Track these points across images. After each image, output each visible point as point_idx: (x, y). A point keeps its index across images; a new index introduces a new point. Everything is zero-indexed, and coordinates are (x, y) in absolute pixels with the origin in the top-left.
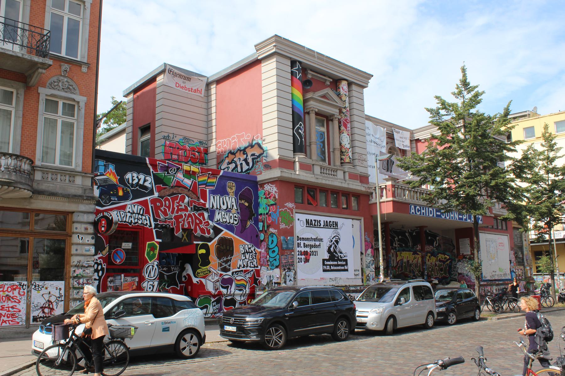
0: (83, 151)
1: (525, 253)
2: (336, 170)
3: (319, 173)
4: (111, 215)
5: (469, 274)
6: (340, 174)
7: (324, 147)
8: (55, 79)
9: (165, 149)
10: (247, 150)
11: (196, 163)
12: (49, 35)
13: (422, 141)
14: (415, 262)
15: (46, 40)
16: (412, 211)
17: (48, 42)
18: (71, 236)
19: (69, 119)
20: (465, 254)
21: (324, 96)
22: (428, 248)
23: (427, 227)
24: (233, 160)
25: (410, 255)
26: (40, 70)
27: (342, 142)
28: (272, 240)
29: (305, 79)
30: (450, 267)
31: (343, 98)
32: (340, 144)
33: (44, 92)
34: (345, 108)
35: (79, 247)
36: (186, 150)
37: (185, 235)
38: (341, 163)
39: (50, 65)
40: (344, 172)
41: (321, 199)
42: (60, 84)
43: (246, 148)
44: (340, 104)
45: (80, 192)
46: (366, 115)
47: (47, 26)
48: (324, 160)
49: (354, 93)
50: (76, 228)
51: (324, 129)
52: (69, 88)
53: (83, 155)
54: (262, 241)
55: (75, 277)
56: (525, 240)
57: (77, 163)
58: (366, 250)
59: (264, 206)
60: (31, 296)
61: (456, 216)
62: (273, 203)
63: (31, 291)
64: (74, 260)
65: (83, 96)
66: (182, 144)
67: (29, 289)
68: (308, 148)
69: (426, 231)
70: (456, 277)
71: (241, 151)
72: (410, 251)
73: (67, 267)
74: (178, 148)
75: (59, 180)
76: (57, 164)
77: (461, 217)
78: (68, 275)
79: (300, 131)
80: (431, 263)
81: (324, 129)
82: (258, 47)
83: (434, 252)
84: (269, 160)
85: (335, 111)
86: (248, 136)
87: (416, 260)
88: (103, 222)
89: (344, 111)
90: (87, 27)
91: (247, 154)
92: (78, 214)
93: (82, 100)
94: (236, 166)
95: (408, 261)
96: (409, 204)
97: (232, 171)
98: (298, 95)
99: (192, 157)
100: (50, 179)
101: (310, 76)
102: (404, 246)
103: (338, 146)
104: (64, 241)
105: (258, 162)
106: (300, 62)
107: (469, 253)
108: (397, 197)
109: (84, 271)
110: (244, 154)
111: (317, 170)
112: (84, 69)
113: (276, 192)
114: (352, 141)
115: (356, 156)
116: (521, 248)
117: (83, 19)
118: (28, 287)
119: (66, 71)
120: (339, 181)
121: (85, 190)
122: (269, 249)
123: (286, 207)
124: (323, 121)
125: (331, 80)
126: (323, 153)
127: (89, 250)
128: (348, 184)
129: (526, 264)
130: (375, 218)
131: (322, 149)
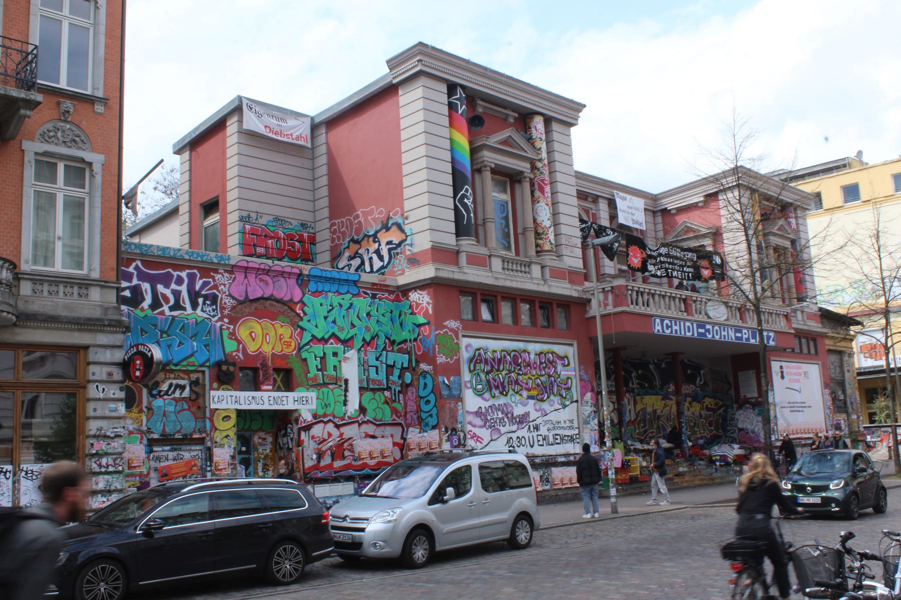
0: (102, 244)
1: (849, 391)
2: (530, 264)
3: (500, 270)
4: (150, 350)
5: (756, 429)
6: (536, 270)
7: (507, 226)
8: (50, 126)
9: (244, 238)
10: (379, 235)
11: (296, 259)
12: (35, 52)
13: (673, 212)
15: (32, 62)
17: (34, 65)
18: (85, 387)
19: (76, 192)
20: (749, 396)
21: (505, 142)
22: (687, 389)
23: (682, 353)
24: (357, 253)
26: (22, 112)
27: (537, 217)
28: (425, 384)
29: (472, 115)
30: (725, 419)
31: (538, 144)
32: (535, 220)
33: (32, 147)
34: (540, 160)
35: (99, 405)
36: (279, 239)
37: (279, 380)
38: (537, 252)
39: (39, 103)
40: (543, 267)
41: (505, 310)
42: (59, 134)
43: (377, 232)
44: (530, 154)
45: (97, 314)
46: (576, 172)
47: (35, 38)
48: (508, 248)
49: (556, 136)
50: (94, 374)
51: (506, 197)
52: (74, 141)
53: (101, 251)
54: (408, 385)
55: (93, 455)
56: (848, 371)
57: (92, 267)
58: (583, 395)
59: (410, 326)
60: (19, 490)
61: (732, 334)
62: (425, 321)
63: (19, 481)
64: (93, 427)
65: (99, 153)
66: (272, 229)
67: (17, 478)
68: (480, 229)
69: (682, 362)
70: (735, 435)
71: (369, 236)
73: (79, 439)
74: (266, 236)
75: (61, 294)
76: (59, 266)
77: (739, 335)
78: (81, 452)
79: (466, 200)
80: (693, 414)
81: (506, 197)
82: (393, 63)
84: (416, 249)
85: (524, 167)
86: (381, 213)
87: (668, 408)
88: (138, 362)
89: (539, 165)
90: (102, 38)
91: (379, 241)
92: (96, 349)
93: (96, 159)
94: (363, 263)
95: (655, 411)
96: (651, 316)
97: (356, 270)
98: (463, 142)
99: (289, 250)
100: (46, 293)
101: (480, 110)
102: (648, 386)
103: (531, 224)
104: (74, 395)
105: (398, 254)
106: (463, 87)
107: (756, 395)
108: (632, 306)
109: (109, 444)
110: (375, 242)
111: (497, 264)
112: (99, 108)
113: (428, 303)
114: (555, 214)
115: (563, 240)
116: (842, 384)
117: (95, 24)
118: (15, 474)
119: (68, 112)
120: (533, 281)
121: (107, 309)
122: (421, 398)
123: (446, 327)
124: (504, 183)
125: (517, 115)
126: (507, 235)
127: (116, 410)
128: (550, 286)
129: (850, 410)
130: (593, 341)
131: (504, 232)
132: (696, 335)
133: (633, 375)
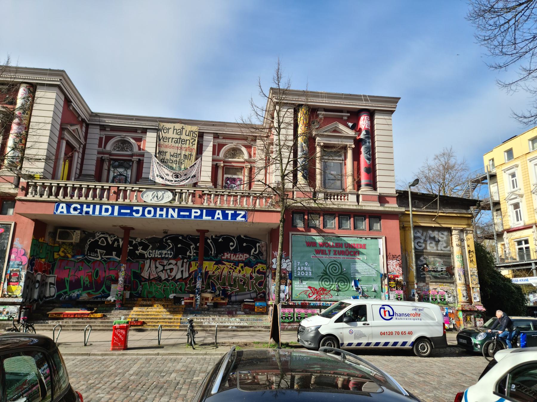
14: (217, 273)
16: (60, 210)
25: (210, 265)
72: (211, 260)
83: (250, 262)
87: (219, 270)
132: (116, 213)
133: (191, 247)
